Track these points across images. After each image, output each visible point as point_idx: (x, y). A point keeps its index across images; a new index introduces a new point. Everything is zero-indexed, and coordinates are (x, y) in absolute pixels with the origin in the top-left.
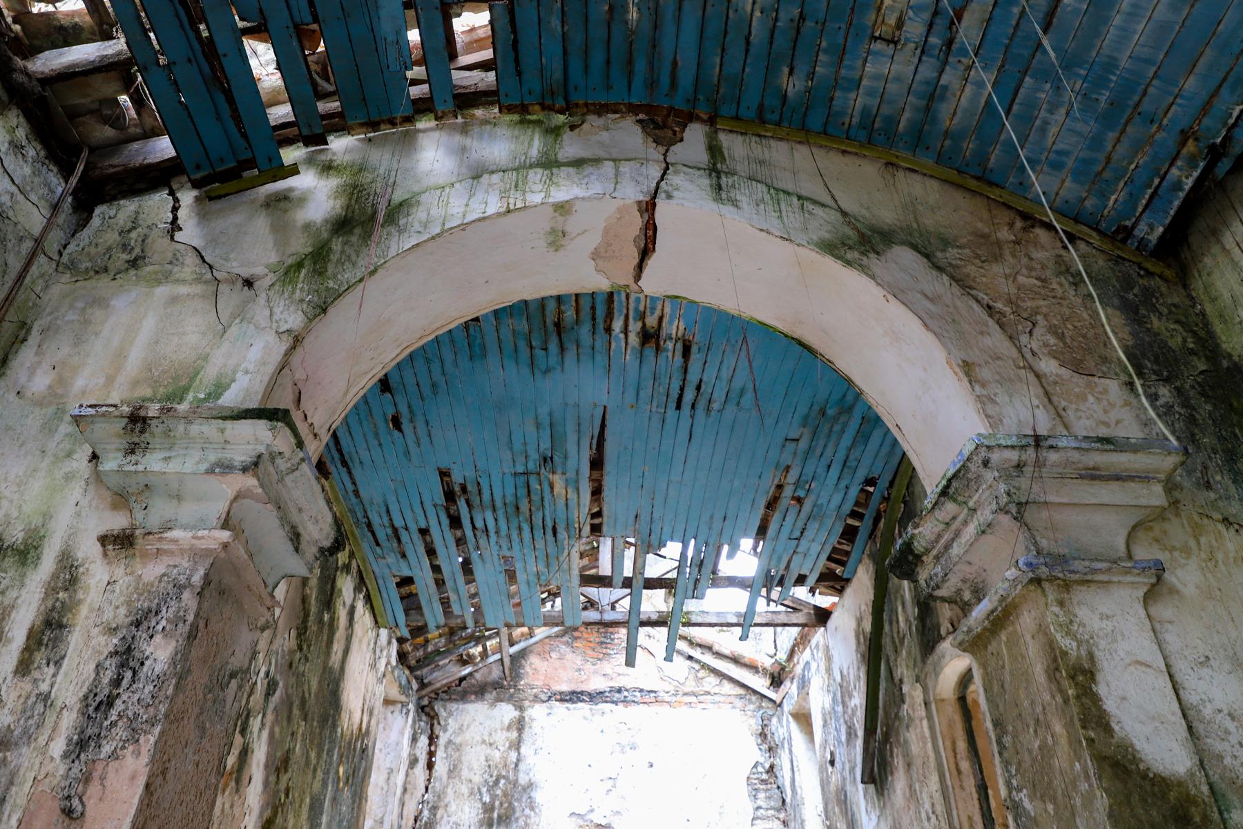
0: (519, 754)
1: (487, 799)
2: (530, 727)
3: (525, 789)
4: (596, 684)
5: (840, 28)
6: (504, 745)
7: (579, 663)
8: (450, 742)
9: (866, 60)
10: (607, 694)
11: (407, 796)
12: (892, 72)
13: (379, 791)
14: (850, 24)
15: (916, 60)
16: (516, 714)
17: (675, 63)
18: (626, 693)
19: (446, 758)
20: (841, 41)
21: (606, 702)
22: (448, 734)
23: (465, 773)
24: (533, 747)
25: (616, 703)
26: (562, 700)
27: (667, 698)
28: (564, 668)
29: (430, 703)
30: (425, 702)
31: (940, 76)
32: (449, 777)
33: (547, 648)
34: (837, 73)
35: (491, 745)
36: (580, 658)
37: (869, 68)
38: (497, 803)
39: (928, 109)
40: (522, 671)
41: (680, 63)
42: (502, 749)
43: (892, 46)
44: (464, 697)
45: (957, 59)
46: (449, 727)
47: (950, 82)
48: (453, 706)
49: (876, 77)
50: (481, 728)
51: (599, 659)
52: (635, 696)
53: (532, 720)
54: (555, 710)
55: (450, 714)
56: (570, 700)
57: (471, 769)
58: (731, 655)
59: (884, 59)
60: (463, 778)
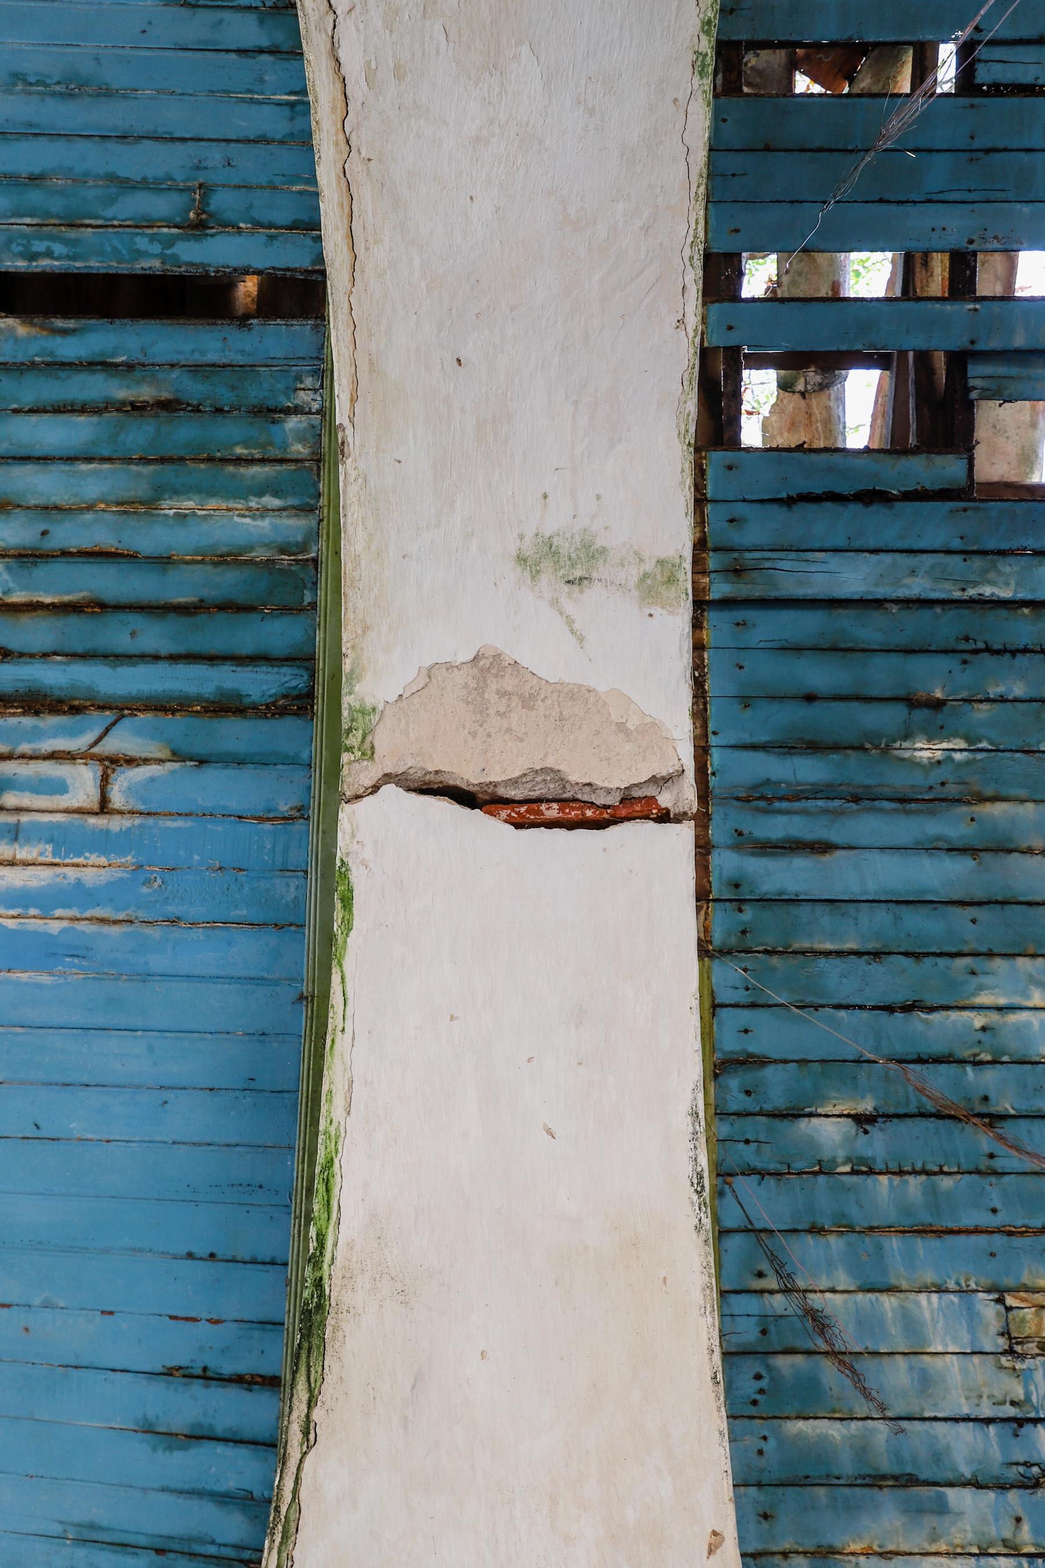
5: (994, 1211)
9: (941, 1290)
12: (938, 1362)
14: (1010, 1234)
15: (987, 1411)
17: (823, 847)
20: (968, 1220)
31: (965, 1484)
34: (887, 1229)
37: (927, 1304)
39: (876, 1481)
41: (826, 858)
43: (1002, 1343)
45: (1020, 1512)
47: (960, 1514)
49: (911, 1324)
59: (965, 1336)
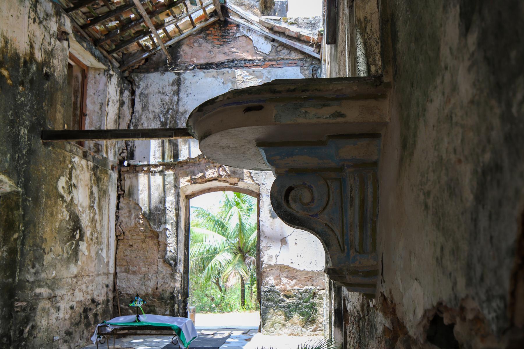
0: (179, 97)
1: (163, 120)
2: (184, 83)
3: (182, 114)
4: (220, 58)
6: (170, 93)
7: (210, 48)
8: (141, 93)
10: (226, 63)
11: (121, 120)
13: (96, 114)
16: (176, 77)
18: (236, 62)
19: (140, 101)
21: (226, 68)
22: (140, 89)
23: (151, 108)
24: (186, 93)
25: (231, 68)
26: (201, 68)
27: (260, 64)
28: (202, 51)
29: (129, 74)
30: (126, 74)
32: (142, 111)
33: (192, 41)
35: (163, 93)
36: (210, 45)
38: (168, 121)
40: (178, 55)
42: (169, 95)
44: (148, 71)
46: (140, 86)
48: (142, 75)
50: (158, 85)
51: (221, 45)
52: (242, 63)
53: (185, 79)
54: (197, 74)
55: (141, 79)
56: (206, 68)
57: (154, 106)
58: (296, 36)
60: (150, 110)
